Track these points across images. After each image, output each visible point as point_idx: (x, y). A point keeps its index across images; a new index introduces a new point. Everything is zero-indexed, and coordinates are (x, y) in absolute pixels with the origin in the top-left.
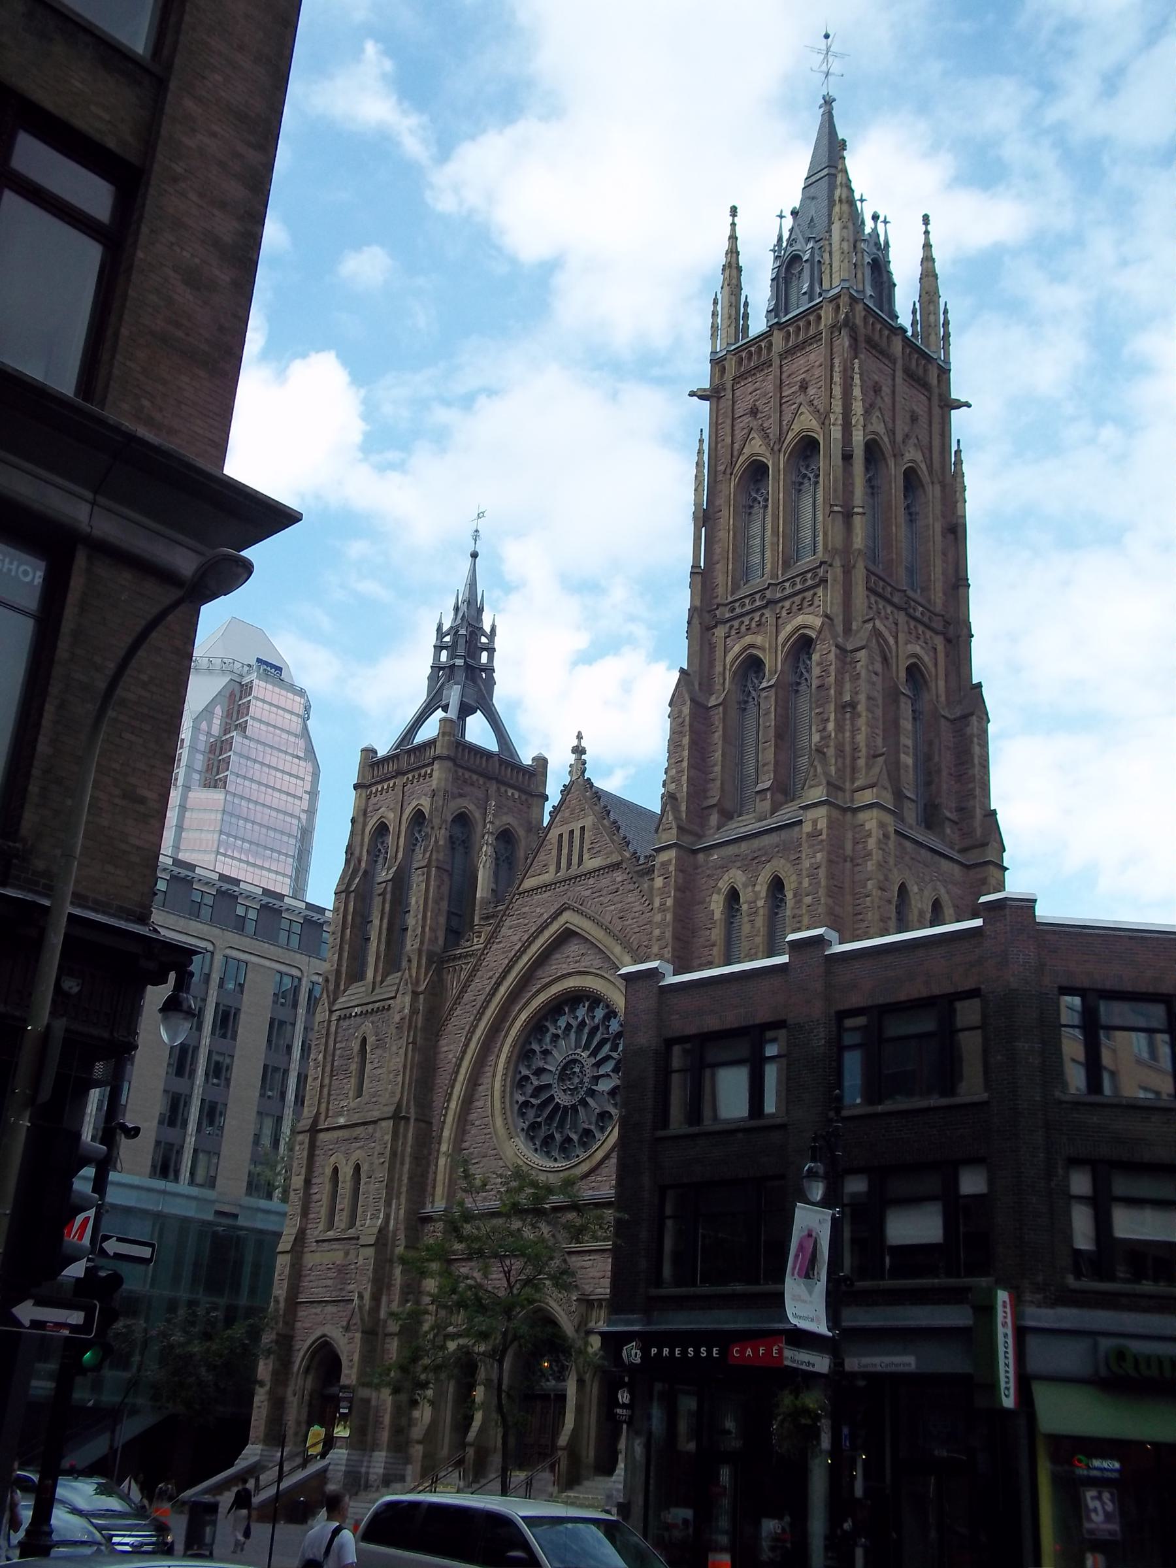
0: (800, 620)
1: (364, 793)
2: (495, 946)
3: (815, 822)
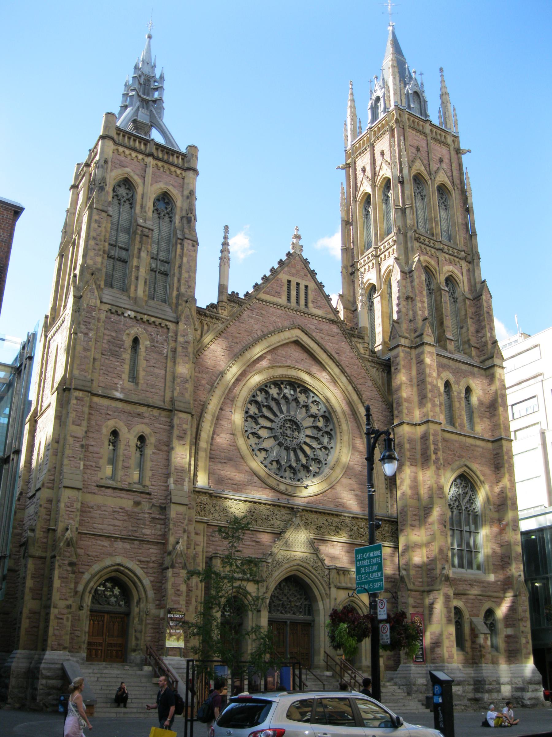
0: (451, 268)
2: (237, 323)
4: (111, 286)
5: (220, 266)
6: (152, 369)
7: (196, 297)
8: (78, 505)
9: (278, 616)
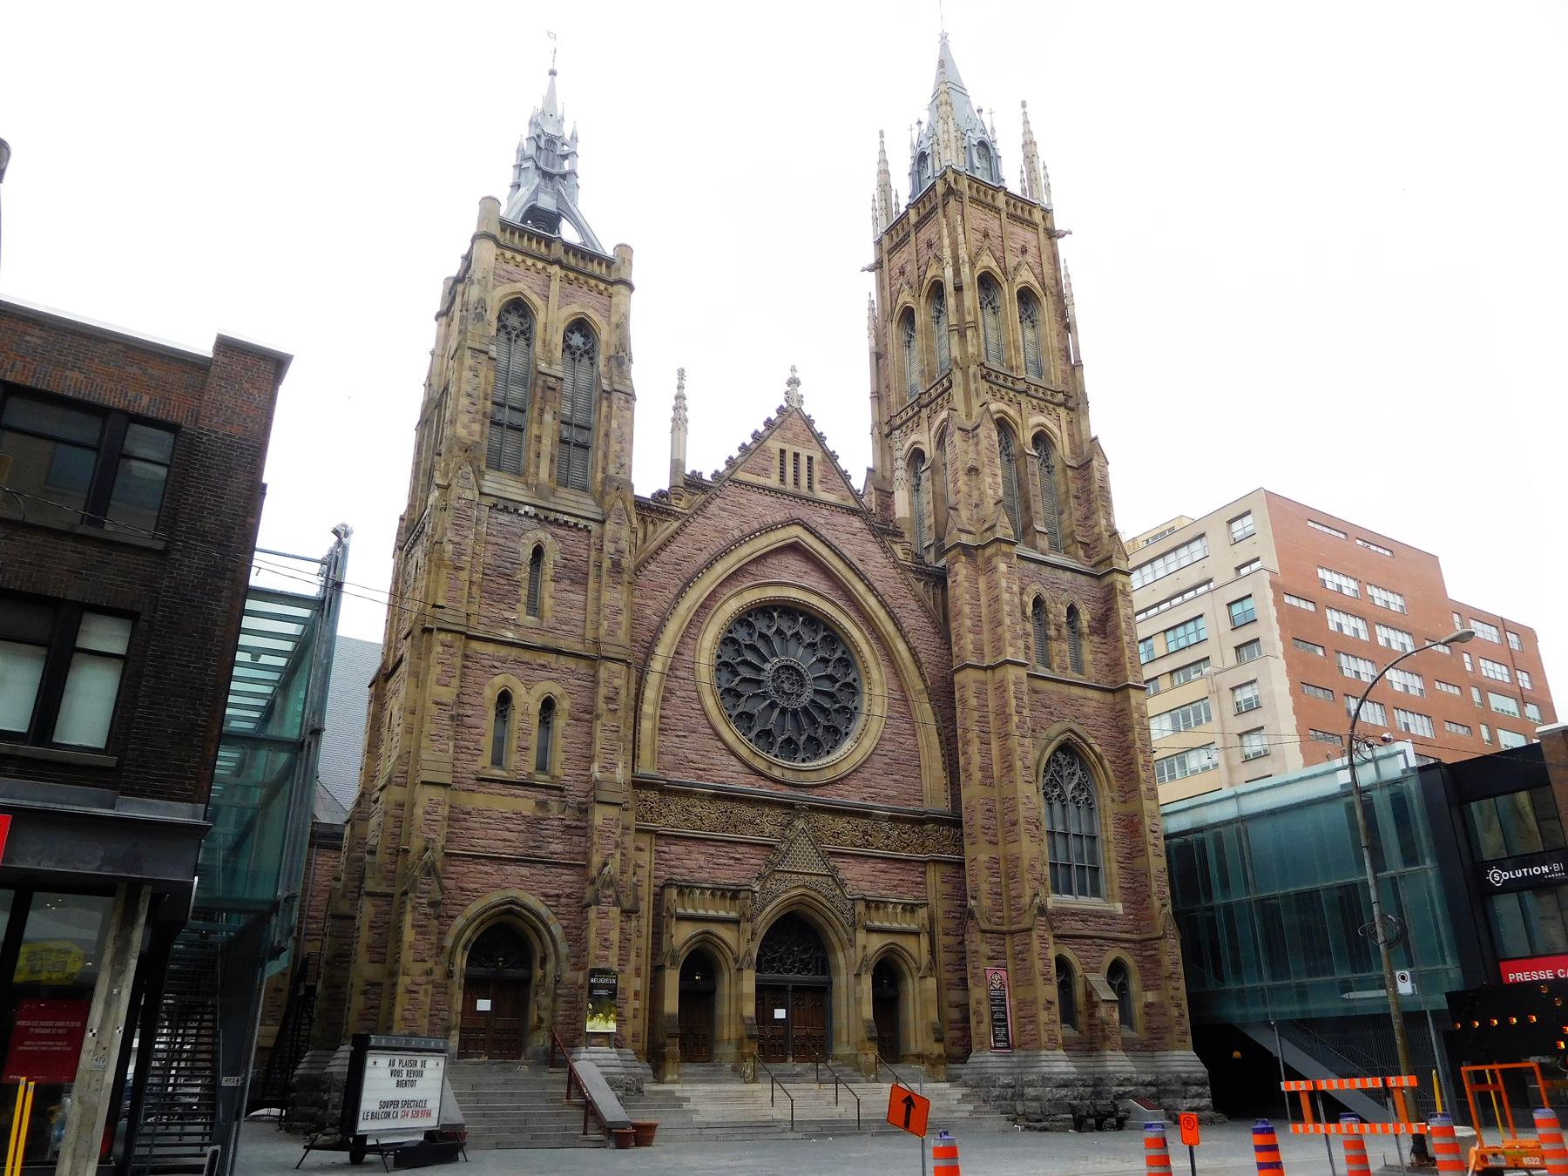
0: (1041, 419)
2: (700, 519)
4: (499, 469)
5: (673, 431)
6: (564, 595)
7: (634, 480)
8: (445, 811)
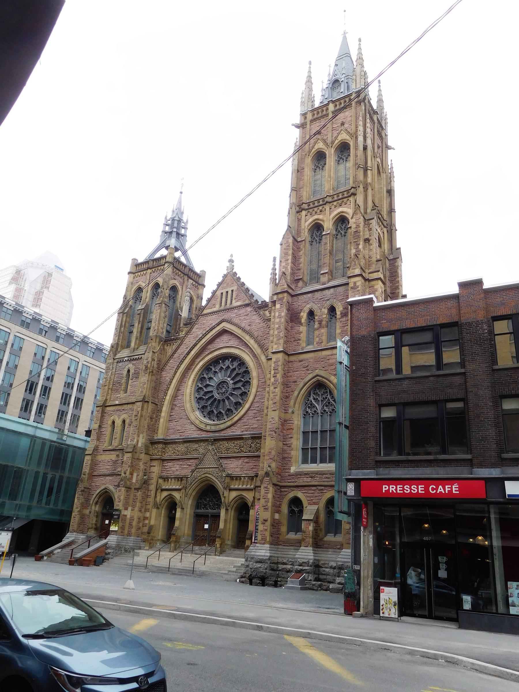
0: (340, 209)
1: (132, 275)
2: (189, 336)
3: (355, 283)
8: (89, 462)
9: (202, 511)
